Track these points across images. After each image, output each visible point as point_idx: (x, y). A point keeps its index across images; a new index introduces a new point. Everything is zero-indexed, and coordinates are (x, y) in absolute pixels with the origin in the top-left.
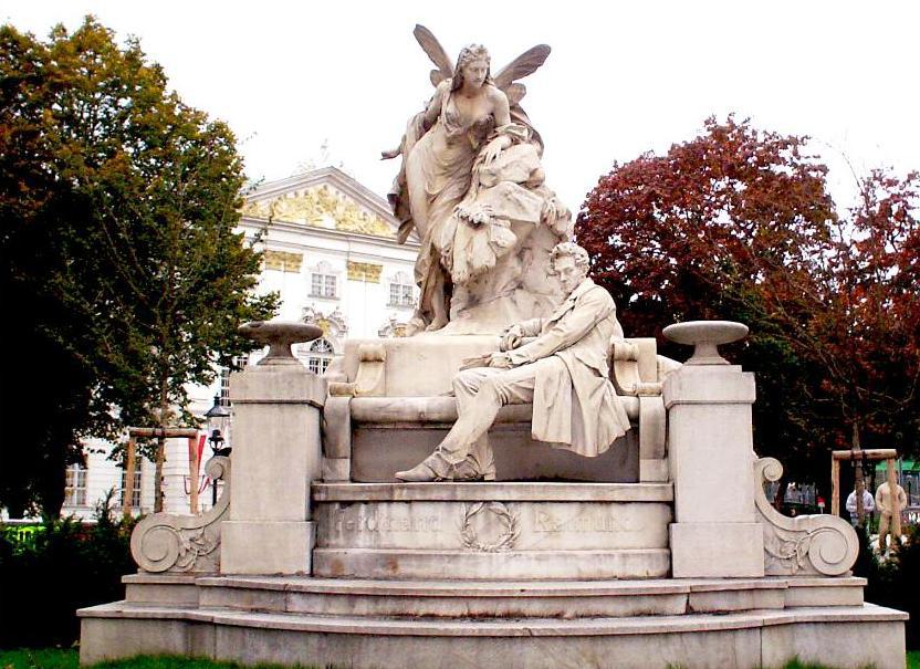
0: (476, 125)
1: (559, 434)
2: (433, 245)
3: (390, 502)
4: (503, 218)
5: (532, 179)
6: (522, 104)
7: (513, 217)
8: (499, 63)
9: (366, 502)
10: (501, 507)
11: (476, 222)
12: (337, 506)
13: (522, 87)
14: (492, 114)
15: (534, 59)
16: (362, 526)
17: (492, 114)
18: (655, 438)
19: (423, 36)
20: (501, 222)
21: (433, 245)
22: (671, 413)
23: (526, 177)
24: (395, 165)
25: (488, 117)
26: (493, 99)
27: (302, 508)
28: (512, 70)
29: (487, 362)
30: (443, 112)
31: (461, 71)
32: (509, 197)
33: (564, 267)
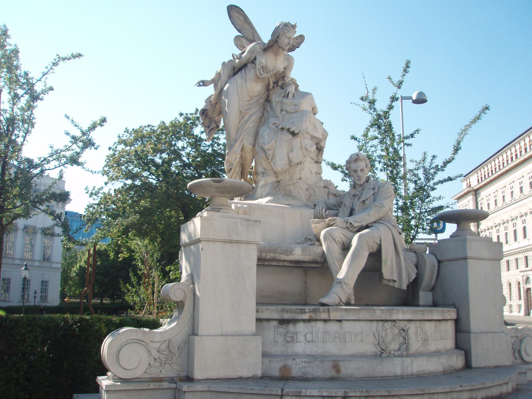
1: (392, 274)
2: (243, 145)
3: (325, 321)
7: (311, 133)
9: (304, 321)
10: (402, 324)
11: (296, 132)
12: (275, 323)
14: (285, 69)
16: (301, 338)
17: (285, 69)
18: (431, 279)
19: (235, 13)
21: (243, 145)
22: (442, 265)
24: (210, 91)
27: (252, 326)
29: (331, 224)
30: (257, 62)
31: (278, 37)
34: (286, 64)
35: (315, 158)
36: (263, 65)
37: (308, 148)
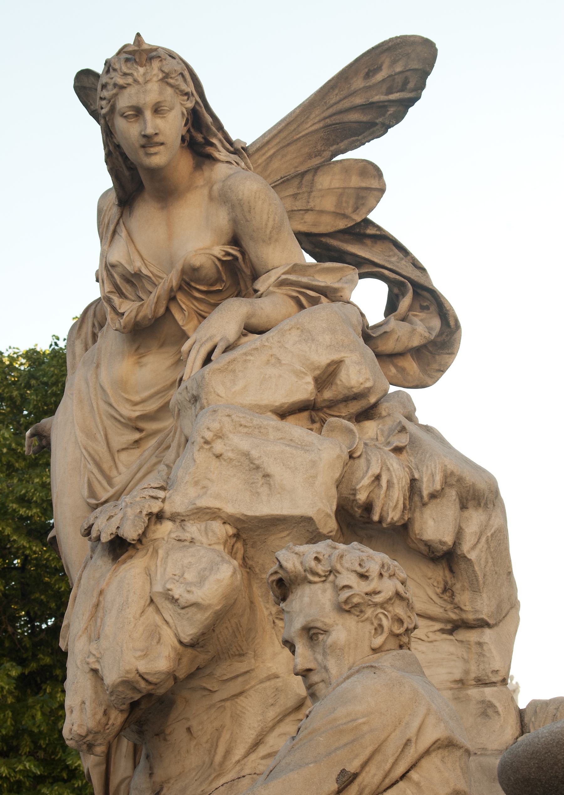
0: (190, 280)
4: (213, 514)
5: (328, 394)
6: (382, 216)
7: (230, 509)
8: (251, 104)
13: (371, 171)
14: (235, 241)
15: (386, 82)
20: (193, 529)
23: (304, 390)
25: (218, 251)
26: (224, 198)
28: (312, 125)
32: (219, 447)
33: (298, 623)
34: (222, 219)
35: (436, 610)
36: (120, 270)
37: (177, 592)
